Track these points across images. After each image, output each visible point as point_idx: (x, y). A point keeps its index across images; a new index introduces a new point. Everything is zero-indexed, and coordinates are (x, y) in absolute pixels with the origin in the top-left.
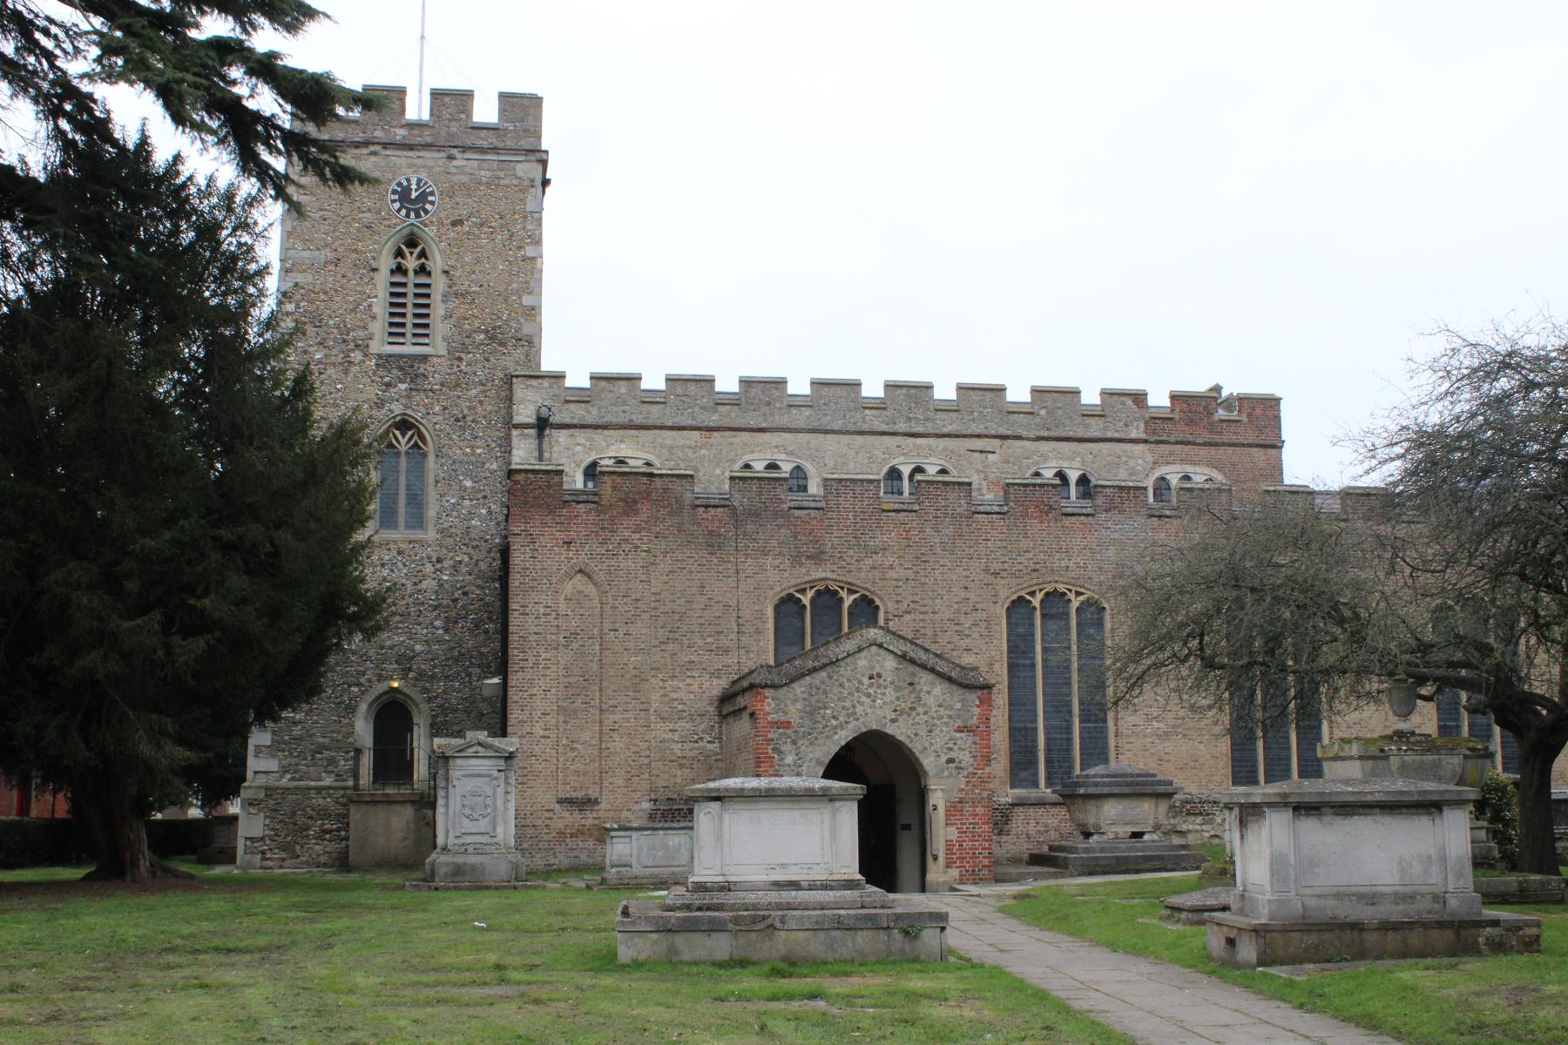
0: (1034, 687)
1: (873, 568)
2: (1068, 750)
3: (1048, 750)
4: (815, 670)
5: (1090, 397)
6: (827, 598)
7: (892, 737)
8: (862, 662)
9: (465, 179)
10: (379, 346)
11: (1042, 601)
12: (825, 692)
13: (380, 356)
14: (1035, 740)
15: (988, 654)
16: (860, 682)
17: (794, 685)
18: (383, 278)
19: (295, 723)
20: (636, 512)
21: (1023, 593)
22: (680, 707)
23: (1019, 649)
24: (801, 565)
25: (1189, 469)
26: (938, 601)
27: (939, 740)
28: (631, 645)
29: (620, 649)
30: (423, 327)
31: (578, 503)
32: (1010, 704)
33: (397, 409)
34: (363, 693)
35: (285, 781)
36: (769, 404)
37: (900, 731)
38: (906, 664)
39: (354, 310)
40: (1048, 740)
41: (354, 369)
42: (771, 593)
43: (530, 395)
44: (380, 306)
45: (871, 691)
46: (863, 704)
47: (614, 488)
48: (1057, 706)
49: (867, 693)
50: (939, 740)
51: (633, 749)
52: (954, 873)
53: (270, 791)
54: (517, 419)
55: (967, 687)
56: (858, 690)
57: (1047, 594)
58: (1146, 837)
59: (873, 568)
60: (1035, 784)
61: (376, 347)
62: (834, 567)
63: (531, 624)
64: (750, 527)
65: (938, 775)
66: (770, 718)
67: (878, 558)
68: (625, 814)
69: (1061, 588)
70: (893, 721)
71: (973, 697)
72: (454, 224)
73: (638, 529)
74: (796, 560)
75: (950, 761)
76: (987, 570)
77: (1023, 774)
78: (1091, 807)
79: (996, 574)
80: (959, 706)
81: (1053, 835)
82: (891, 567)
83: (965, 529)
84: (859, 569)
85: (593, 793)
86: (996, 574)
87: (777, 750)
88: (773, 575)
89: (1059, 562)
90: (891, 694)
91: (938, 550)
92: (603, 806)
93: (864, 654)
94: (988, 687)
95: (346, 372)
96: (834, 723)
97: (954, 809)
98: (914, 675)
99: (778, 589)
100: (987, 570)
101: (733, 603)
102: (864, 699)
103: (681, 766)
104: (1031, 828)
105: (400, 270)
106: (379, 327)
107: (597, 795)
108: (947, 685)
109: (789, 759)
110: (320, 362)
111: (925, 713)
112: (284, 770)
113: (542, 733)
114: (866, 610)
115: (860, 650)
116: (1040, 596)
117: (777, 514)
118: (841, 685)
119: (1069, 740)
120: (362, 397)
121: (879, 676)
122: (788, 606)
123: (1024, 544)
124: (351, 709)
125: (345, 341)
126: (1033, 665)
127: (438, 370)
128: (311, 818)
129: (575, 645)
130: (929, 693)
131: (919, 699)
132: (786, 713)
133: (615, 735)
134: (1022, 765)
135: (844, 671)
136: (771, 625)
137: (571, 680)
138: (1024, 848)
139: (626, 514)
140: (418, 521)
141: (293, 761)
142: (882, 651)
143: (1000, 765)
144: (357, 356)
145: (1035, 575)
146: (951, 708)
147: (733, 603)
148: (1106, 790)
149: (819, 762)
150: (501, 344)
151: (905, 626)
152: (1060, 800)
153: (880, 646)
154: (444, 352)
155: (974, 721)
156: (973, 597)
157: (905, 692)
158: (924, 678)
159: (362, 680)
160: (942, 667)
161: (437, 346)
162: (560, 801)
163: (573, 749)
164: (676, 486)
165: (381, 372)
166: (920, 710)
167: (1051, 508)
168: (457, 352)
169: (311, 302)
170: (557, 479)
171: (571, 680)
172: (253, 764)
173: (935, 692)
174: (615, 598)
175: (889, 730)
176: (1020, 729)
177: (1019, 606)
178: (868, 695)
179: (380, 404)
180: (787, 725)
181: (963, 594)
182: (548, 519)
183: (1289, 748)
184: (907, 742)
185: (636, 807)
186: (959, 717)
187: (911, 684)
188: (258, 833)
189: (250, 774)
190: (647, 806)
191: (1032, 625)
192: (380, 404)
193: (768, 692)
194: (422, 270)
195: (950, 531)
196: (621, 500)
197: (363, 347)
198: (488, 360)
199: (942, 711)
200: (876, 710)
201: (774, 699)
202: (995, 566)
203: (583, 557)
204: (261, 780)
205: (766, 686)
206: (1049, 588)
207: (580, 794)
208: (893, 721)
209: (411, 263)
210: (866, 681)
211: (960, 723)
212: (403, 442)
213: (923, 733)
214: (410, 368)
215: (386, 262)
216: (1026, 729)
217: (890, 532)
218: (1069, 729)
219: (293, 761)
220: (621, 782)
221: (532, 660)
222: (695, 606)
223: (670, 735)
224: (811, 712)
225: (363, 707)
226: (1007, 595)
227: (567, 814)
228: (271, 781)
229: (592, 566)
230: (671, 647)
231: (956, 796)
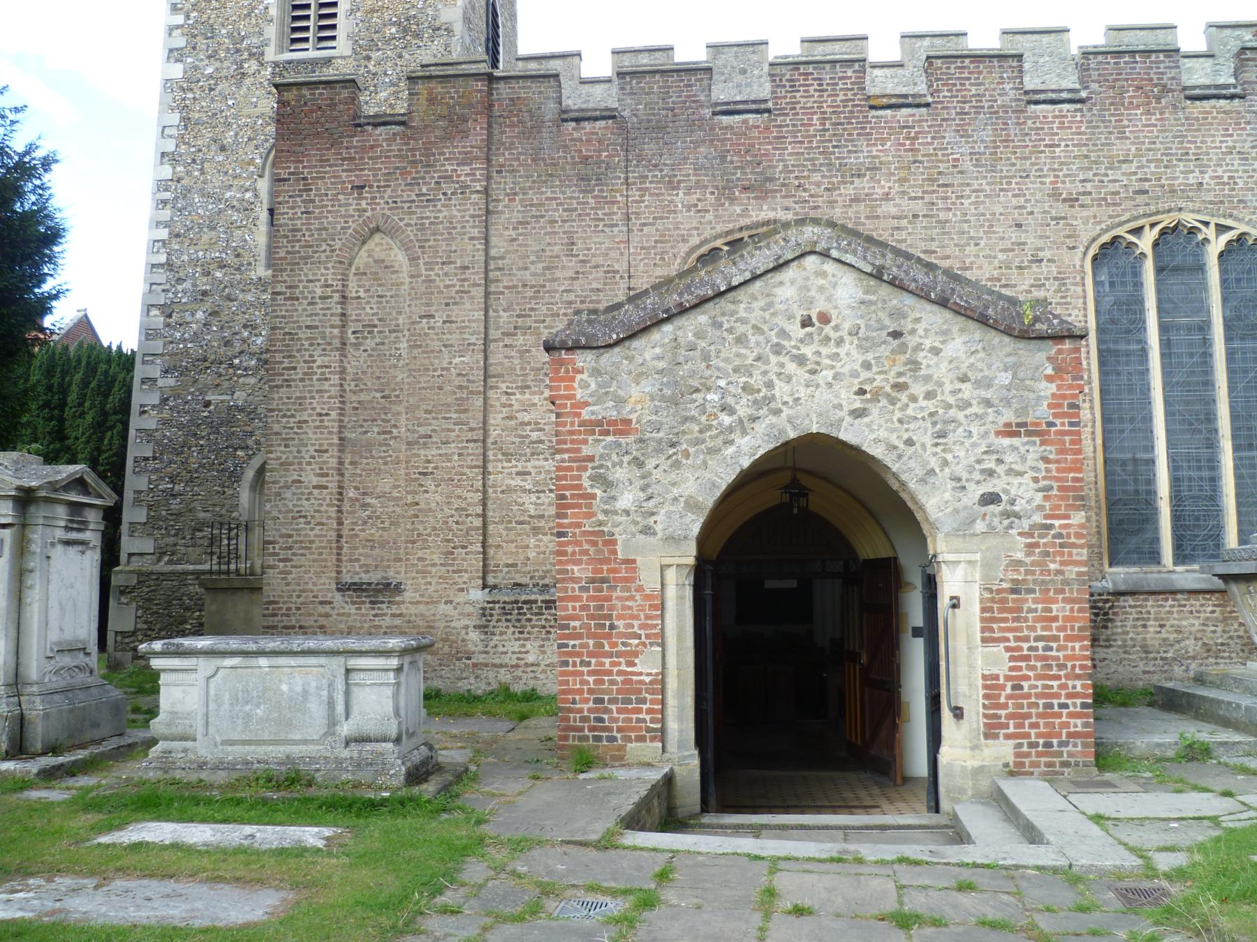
0: (1146, 390)
1: (856, 200)
4: (683, 311)
5: (1191, 39)
7: (856, 450)
8: (786, 288)
11: (1156, 244)
12: (706, 357)
13: (276, 64)
14: (1151, 481)
16: (783, 333)
17: (636, 343)
19: (174, 496)
20: (465, 134)
21: (1119, 231)
22: (535, 436)
24: (732, 200)
26: (971, 249)
27: (962, 455)
28: (454, 338)
29: (436, 345)
31: (376, 125)
32: (1106, 420)
34: (250, 457)
35: (162, 567)
36: (744, 72)
37: (870, 435)
38: (885, 290)
39: (249, 15)
40: (1175, 482)
41: (248, 81)
42: (684, 248)
45: (808, 351)
46: (789, 379)
47: (432, 100)
48: (1192, 419)
49: (804, 365)
50: (962, 455)
51: (457, 503)
52: (1003, 750)
53: (144, 576)
55: (1025, 335)
56: (778, 350)
57: (1163, 233)
59: (856, 200)
60: (1154, 556)
61: (271, 54)
62: (789, 202)
64: (649, 148)
65: (964, 530)
66: (586, 414)
67: (864, 184)
68: (442, 608)
69: (1190, 219)
70: (858, 414)
71: (1039, 357)
75: (990, 499)
76: (1055, 195)
79: (1071, 201)
80: (1005, 378)
81: (1191, 645)
82: (887, 197)
83: (1013, 131)
84: (832, 203)
85: (393, 576)
86: (1071, 201)
87: (606, 483)
88: (687, 220)
89: (1182, 176)
90: (851, 356)
91: (968, 165)
92: (408, 595)
93: (791, 273)
95: (239, 85)
96: (727, 420)
97: (1001, 607)
98: (898, 314)
99: (695, 241)
100: (1055, 195)
101: (621, 266)
102: (791, 367)
103: (536, 531)
107: (399, 578)
108: (977, 332)
109: (626, 500)
110: (211, 77)
111: (929, 395)
112: (160, 553)
113: (315, 480)
115: (779, 267)
116: (1150, 236)
117: (691, 125)
118: (740, 340)
119: (1214, 481)
120: (258, 111)
121: (825, 318)
123: (1119, 148)
124: (235, 477)
125: (238, 51)
126: (1144, 353)
128: (188, 609)
129: (370, 343)
130: (936, 351)
131: (914, 365)
132: (620, 401)
133: (429, 483)
135: (747, 307)
137: (363, 397)
139: (447, 137)
141: (171, 540)
142: (830, 267)
144: (251, 66)
145: (1141, 199)
146: (986, 383)
147: (621, 266)
149: (691, 505)
150: (418, 36)
152: (1219, 584)
153: (825, 255)
154: (349, 53)
155: (1043, 412)
156: (1031, 240)
157: (884, 351)
158: (927, 320)
159: (250, 442)
161: (342, 46)
162: (342, 588)
163: (365, 506)
164: (531, 92)
166: (918, 389)
167: (1165, 90)
169: (201, 12)
170: (345, 94)
171: (363, 397)
173: (949, 347)
174: (430, 266)
175: (849, 433)
176: (1124, 463)
178: (801, 360)
180: (622, 427)
181: (1014, 236)
182: (330, 155)
184: (888, 459)
185: (461, 598)
186: (1007, 402)
187: (896, 335)
188: (130, 627)
189: (123, 557)
190: (477, 595)
191: (1139, 285)
193: (583, 359)
195: (987, 134)
196: (442, 117)
197: (258, 55)
198: (400, 57)
199: (967, 390)
200: (817, 399)
201: (596, 372)
202: (1069, 188)
203: (382, 207)
204: (136, 564)
205: (577, 347)
206: (1167, 221)
207: (374, 577)
208: (858, 414)
210: (797, 331)
211: (1009, 416)
213: (822, 282)
216: (1135, 460)
217: (883, 141)
218: (1213, 463)
219: (171, 540)
220: (436, 558)
221: (302, 368)
222: (558, 274)
223: (518, 481)
224: (676, 395)
226: (1091, 228)
227: (352, 609)
228: (146, 565)
230: (520, 340)
231: (1003, 577)
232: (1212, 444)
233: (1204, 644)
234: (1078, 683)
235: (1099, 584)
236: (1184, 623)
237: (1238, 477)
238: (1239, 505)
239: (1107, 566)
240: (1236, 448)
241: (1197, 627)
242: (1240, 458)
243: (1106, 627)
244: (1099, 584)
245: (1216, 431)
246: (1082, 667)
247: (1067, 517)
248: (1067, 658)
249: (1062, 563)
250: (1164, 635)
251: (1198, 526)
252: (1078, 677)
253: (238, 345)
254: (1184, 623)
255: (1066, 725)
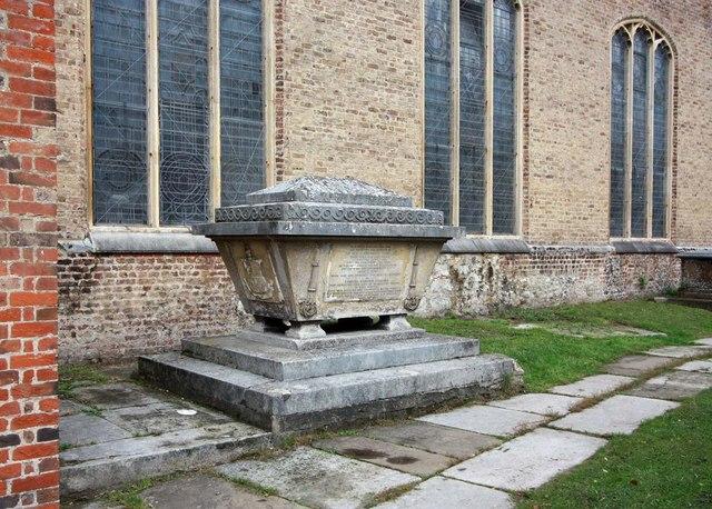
2: (201, 158)
3: (166, 157)
14: (142, 134)
32: (97, 60)
58: (392, 324)
77: (120, 198)
78: (299, 263)
104: (136, 301)
119: (202, 143)
138: (119, 337)
148: (335, 229)
152: (210, 245)
176: (113, 112)
183: (483, 184)
216: (126, 112)
232: (202, 107)
233: (187, 307)
234: (36, 403)
235: (80, 243)
236: (169, 285)
237: (224, 141)
238: (223, 169)
239: (91, 223)
240: (224, 112)
241: (181, 289)
242: (227, 123)
243: (87, 291)
244: (80, 243)
245: (207, 92)
246: (42, 375)
247: (26, 133)
248: (17, 362)
249: (13, 208)
250: (149, 299)
251: (185, 187)
252: (36, 391)
254: (169, 285)
255: (15, 470)
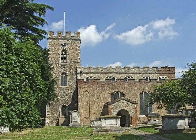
6: (117, 93)
8: (121, 101)
9: (70, 43)
10: (60, 63)
15: (137, 100)
18: (60, 55)
23: (141, 99)
25: (163, 76)
30: (66, 62)
33: (63, 71)
37: (126, 109)
43: (79, 69)
44: (60, 59)
53: (49, 117)
54: (78, 72)
55: (135, 104)
63: (80, 97)
72: (69, 48)
73: (94, 86)
74: (113, 89)
76: (137, 90)
86: (138, 90)
94: (137, 104)
100: (137, 90)
105: (62, 54)
106: (60, 61)
114: (122, 94)
122: (112, 94)
127: (68, 66)
134: (141, 113)
136: (110, 97)
140: (66, 84)
143: (138, 113)
144: (57, 65)
151: (126, 97)
160: (131, 101)
165: (61, 67)
168: (70, 64)
172: (47, 113)
177: (141, 94)
179: (61, 71)
192: (61, 71)
194: (65, 54)
204: (48, 115)
209: (64, 53)
212: (64, 75)
214: (64, 66)
215: (61, 53)
225: (60, 107)
228: (49, 115)
229: (88, 90)
253: (58, 94)
